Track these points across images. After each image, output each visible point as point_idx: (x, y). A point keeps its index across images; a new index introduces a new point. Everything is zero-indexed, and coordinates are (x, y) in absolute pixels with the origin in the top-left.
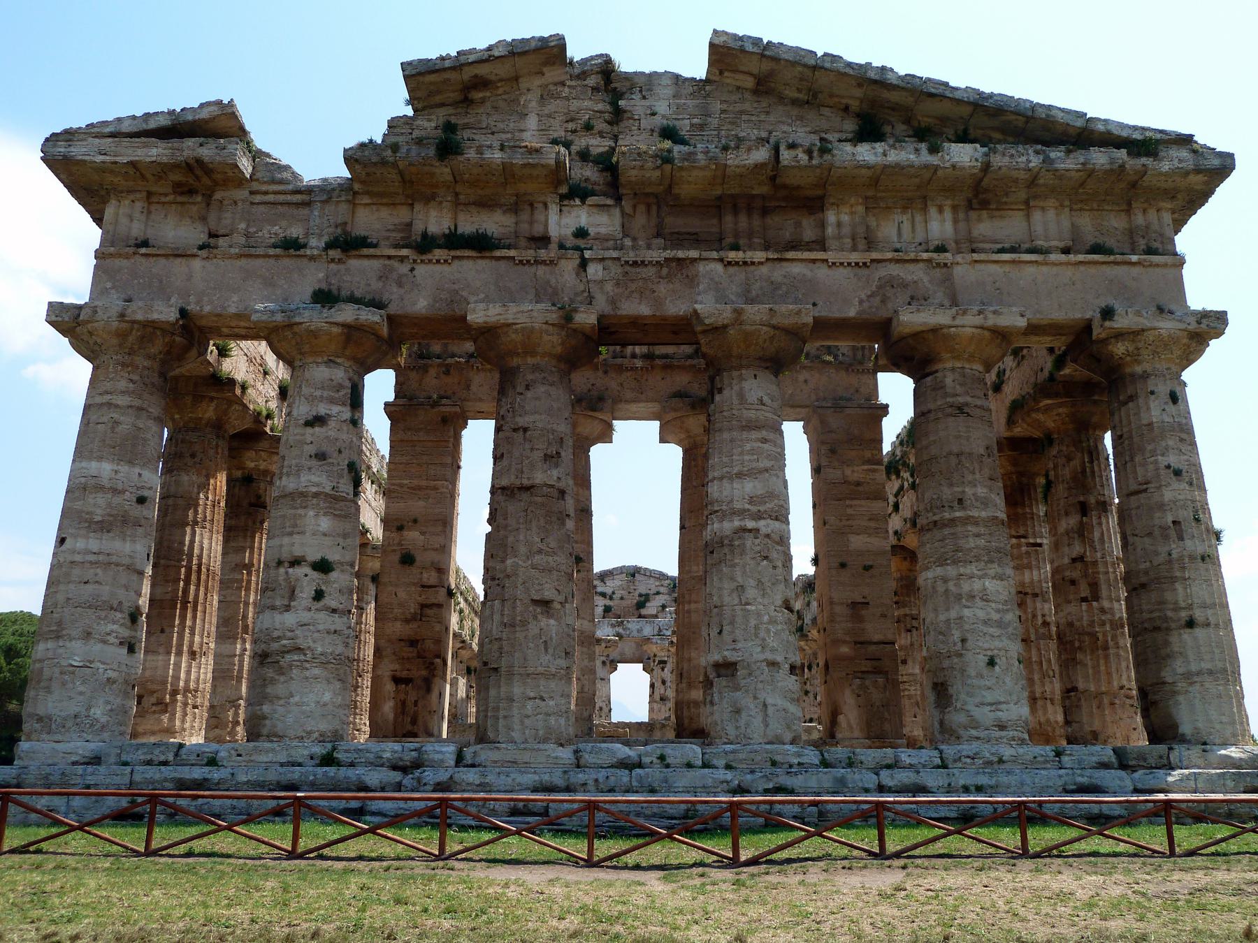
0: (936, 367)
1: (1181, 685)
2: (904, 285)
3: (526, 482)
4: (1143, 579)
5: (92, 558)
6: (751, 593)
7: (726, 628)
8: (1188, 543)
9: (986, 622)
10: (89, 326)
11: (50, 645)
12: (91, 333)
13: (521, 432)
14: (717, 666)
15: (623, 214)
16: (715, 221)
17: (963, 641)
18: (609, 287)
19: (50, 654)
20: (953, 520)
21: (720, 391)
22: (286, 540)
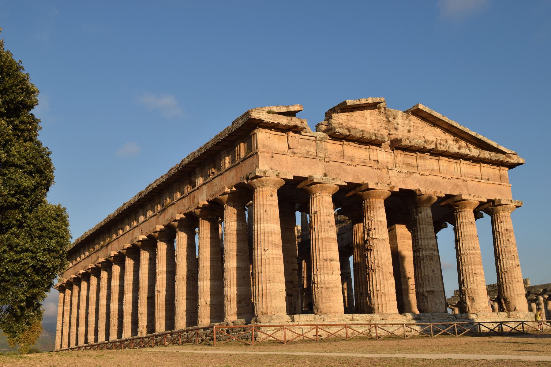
0: (465, 210)
1: (516, 297)
2: (458, 186)
3: (384, 238)
4: (506, 270)
5: (278, 256)
6: (436, 272)
7: (431, 281)
8: (516, 261)
9: (482, 281)
10: (268, 178)
11: (272, 284)
12: (267, 180)
13: (379, 223)
14: (427, 292)
15: (394, 156)
16: (415, 161)
17: (477, 285)
18: (395, 179)
19: (272, 287)
20: (473, 253)
21: (420, 213)
22: (328, 252)
